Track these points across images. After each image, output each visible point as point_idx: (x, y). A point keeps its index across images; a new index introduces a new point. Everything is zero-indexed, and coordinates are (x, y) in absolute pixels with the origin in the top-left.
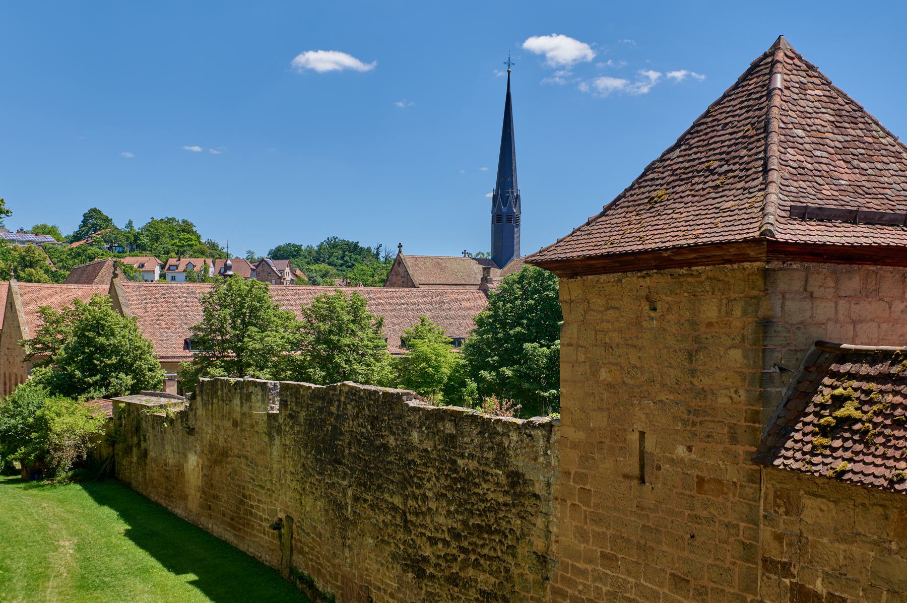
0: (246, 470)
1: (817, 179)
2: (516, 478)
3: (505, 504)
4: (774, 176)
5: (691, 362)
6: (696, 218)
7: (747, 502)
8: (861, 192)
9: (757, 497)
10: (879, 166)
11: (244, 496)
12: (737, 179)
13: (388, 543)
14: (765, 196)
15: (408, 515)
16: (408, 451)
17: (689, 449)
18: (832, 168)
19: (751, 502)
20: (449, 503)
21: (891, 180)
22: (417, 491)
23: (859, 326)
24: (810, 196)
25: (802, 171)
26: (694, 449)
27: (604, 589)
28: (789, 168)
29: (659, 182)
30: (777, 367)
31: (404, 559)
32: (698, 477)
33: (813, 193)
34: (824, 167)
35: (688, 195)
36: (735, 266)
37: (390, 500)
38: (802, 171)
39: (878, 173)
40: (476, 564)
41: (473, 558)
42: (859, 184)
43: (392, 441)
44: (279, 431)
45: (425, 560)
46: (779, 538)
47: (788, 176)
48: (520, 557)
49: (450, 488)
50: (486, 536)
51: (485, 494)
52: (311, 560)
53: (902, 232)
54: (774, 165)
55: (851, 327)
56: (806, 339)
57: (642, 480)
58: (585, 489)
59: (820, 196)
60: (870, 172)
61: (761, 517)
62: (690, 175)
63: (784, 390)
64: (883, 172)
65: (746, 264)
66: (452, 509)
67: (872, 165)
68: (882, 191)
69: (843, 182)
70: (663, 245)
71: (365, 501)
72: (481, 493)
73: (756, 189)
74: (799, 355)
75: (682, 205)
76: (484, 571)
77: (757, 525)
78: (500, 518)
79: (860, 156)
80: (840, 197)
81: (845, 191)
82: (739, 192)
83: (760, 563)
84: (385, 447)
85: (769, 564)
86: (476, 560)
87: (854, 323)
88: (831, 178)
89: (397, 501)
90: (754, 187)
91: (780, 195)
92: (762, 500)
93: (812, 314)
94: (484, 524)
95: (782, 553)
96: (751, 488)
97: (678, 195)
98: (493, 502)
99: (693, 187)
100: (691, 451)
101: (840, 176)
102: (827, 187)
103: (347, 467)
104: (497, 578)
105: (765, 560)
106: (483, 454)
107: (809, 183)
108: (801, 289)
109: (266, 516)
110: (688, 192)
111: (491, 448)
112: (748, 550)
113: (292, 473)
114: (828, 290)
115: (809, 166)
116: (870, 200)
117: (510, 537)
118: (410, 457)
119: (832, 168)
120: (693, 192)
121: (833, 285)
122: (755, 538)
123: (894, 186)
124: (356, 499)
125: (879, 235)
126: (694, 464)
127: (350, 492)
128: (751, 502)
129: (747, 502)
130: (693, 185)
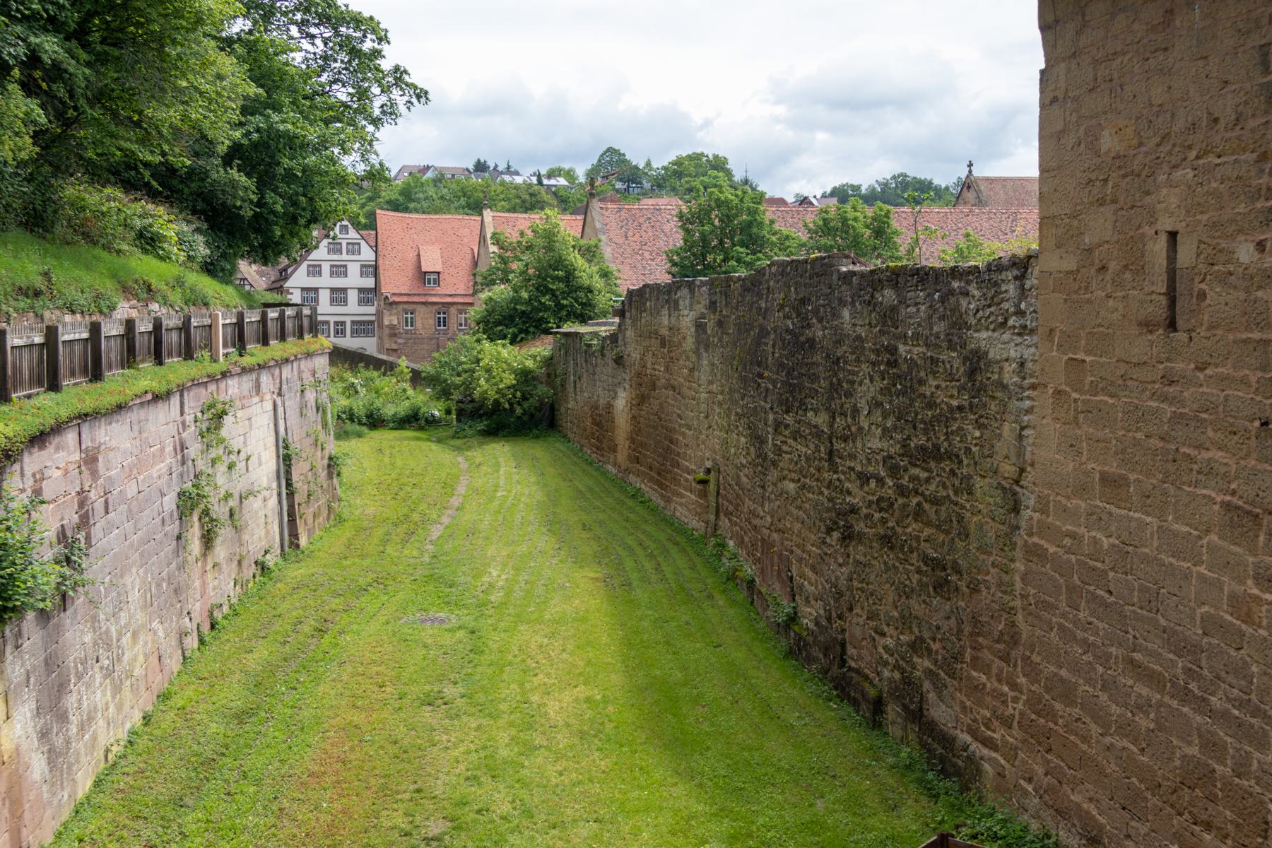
0: (673, 406)
2: (976, 362)
3: (960, 408)
11: (671, 441)
20: (885, 415)
27: (1106, 542)
40: (918, 513)
41: (915, 501)
45: (854, 510)
48: (978, 493)
49: (885, 391)
50: (932, 464)
51: (932, 393)
52: (736, 524)
57: (1172, 325)
58: (1075, 360)
66: (889, 424)
72: (928, 394)
76: (928, 524)
78: (952, 432)
86: (919, 504)
94: (930, 444)
98: (943, 406)
100: (1263, 251)
104: (947, 533)
106: (931, 329)
109: (693, 467)
111: (942, 318)
117: (966, 462)
124: (778, 425)
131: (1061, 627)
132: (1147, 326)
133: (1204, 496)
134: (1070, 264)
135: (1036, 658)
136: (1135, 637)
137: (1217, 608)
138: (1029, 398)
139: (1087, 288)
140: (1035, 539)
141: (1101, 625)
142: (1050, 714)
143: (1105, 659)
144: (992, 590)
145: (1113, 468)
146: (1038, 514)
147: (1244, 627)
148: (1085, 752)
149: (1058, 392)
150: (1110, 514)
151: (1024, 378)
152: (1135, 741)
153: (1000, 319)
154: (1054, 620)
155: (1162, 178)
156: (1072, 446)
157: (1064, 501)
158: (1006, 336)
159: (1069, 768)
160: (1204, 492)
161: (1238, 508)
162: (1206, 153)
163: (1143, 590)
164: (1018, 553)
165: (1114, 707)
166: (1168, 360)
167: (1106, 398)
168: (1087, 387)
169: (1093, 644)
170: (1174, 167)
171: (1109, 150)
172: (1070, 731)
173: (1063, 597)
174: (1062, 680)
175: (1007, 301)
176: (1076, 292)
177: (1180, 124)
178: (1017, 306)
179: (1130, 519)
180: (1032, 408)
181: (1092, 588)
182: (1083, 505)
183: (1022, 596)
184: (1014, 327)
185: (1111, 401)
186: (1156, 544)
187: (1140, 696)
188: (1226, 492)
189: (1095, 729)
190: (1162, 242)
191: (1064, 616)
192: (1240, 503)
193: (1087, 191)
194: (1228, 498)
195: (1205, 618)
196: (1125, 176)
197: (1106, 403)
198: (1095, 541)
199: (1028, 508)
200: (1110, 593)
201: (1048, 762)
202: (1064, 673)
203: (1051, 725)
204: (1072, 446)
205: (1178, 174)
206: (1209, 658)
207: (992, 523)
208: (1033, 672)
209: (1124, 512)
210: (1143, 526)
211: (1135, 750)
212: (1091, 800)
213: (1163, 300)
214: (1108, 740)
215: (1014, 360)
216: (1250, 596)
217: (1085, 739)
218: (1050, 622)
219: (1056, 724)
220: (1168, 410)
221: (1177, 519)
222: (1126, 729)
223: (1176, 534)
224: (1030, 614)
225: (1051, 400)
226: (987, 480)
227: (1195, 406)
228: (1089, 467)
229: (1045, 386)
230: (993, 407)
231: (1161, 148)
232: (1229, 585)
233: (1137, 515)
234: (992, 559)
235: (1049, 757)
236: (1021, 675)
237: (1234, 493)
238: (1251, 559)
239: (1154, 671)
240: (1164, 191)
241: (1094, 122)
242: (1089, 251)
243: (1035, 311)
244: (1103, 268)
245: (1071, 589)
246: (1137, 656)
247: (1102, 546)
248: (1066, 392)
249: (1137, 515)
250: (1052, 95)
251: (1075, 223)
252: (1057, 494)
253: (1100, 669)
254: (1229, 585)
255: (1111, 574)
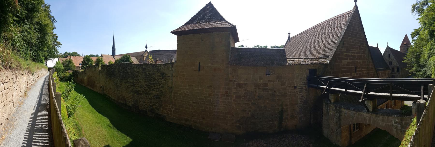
13: (130, 89)
15: (134, 83)
16: (134, 72)
22: (137, 79)
31: (134, 91)
37: (129, 81)
43: (129, 71)
44: (101, 73)
71: (123, 82)
84: (128, 72)
89: (131, 81)
103: (118, 77)
113: (104, 79)
118: (134, 73)
124: (121, 82)
127: (119, 81)
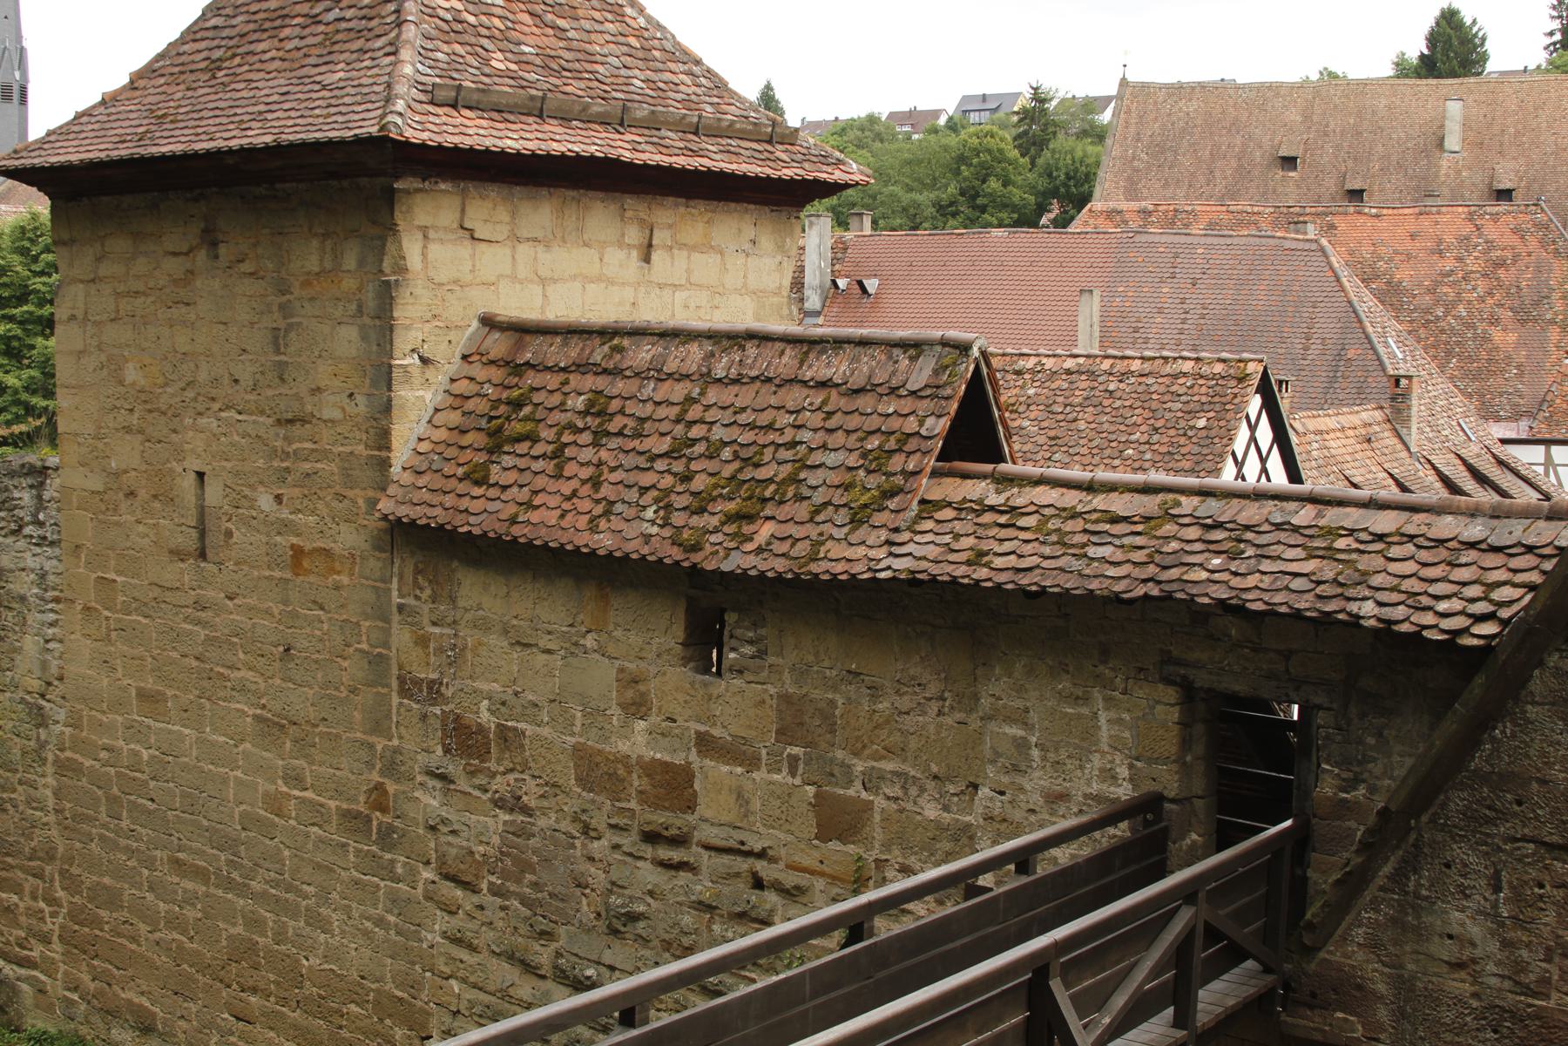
1: (485, 42)
4: (410, 32)
5: (278, 351)
6: (283, 98)
7: (370, 582)
8: (556, 67)
9: (388, 574)
10: (587, 25)
12: (353, 35)
14: (394, 64)
17: (278, 499)
18: (510, 24)
19: (378, 584)
21: (605, 51)
23: (550, 289)
24: (471, 70)
25: (459, 27)
26: (285, 499)
27: (145, 754)
28: (437, 20)
29: (225, 33)
30: (416, 356)
32: (292, 546)
33: (476, 64)
34: (497, 22)
35: (273, 59)
36: (345, 183)
38: (459, 27)
39: (585, 37)
42: (553, 53)
46: (422, 641)
47: (434, 33)
53: (617, 136)
54: (411, 14)
55: (538, 290)
56: (465, 308)
57: (202, 555)
59: (487, 70)
60: (572, 34)
61: (395, 609)
62: (278, 23)
63: (428, 396)
64: (593, 36)
65: (363, 181)
67: (575, 24)
68: (588, 67)
69: (526, 49)
70: (226, 143)
73: (381, 53)
74: (452, 336)
75: (262, 75)
77: (387, 620)
79: (557, 7)
80: (521, 73)
81: (527, 63)
82: (355, 56)
83: (395, 684)
85: (408, 687)
87: (543, 282)
88: (506, 40)
90: (379, 49)
91: (419, 65)
92: (395, 580)
93: (474, 266)
95: (428, 664)
96: (379, 559)
97: (256, 58)
99: (282, 45)
100: (280, 503)
101: (522, 38)
102: (499, 55)
105: (402, 680)
107: (469, 48)
108: (455, 225)
110: (273, 53)
112: (378, 662)
114: (498, 227)
115: (471, 19)
116: (570, 81)
119: (510, 24)
120: (281, 54)
121: (507, 219)
122: (386, 645)
123: (610, 59)
125: (580, 138)
126: (285, 527)
128: (378, 584)
129: (370, 582)
130: (281, 40)
131: (102, 838)
132: (178, 554)
133: (238, 710)
134: (96, 483)
135: (75, 870)
136: (180, 839)
137: (252, 805)
138: (52, 610)
139: (115, 510)
140: (68, 754)
141: (144, 831)
142: (96, 922)
143: (150, 864)
144: (21, 808)
145: (150, 684)
146: (70, 729)
147: (276, 819)
148: (133, 951)
149: (87, 609)
150: (149, 727)
151: (46, 590)
152: (184, 932)
153: (13, 526)
154: (94, 831)
155: (188, 421)
156: (105, 662)
157: (99, 715)
158: (22, 544)
159: (118, 968)
160: (238, 706)
161: (268, 720)
162: (228, 408)
163: (184, 796)
164: (50, 769)
165: (161, 904)
166: (200, 587)
167: (140, 618)
168: (119, 607)
169: (137, 849)
170: (200, 414)
171: (134, 384)
172: (119, 935)
173: (103, 809)
174: (105, 887)
175: (22, 508)
176: (104, 513)
177: (203, 376)
178: (35, 515)
179: (170, 732)
180: (57, 621)
181: (132, 798)
182: (120, 719)
183: (57, 811)
184: (31, 537)
185: (144, 621)
186: (194, 753)
187: (185, 891)
188: (258, 706)
189: (143, 928)
190: (190, 480)
191: (105, 826)
192: (269, 715)
193: (111, 416)
194: (259, 711)
195: (244, 815)
196: (150, 411)
197: (139, 622)
198: (136, 754)
199: (58, 722)
200: (152, 800)
201: (94, 967)
202: (107, 880)
203: (97, 932)
204: (105, 662)
205: (203, 421)
206: (246, 849)
207: (17, 740)
208: (72, 885)
209: (162, 725)
210: (181, 738)
211: (185, 939)
212: (142, 993)
213: (194, 534)
214: (158, 935)
215: (33, 571)
216: (281, 793)
217: (134, 939)
218: (90, 834)
219: (102, 930)
220: (202, 633)
221: (215, 730)
222: (174, 922)
223: (213, 744)
224: (66, 828)
225: (80, 616)
226: (8, 695)
227: (226, 631)
228: (125, 682)
229: (72, 601)
230: (10, 619)
231: (186, 393)
232: (263, 785)
233: (176, 728)
234: (18, 776)
235: (95, 962)
236: (59, 889)
237: (264, 707)
238: (281, 762)
239: (197, 867)
240: (191, 434)
241: (116, 351)
242: (117, 475)
243: (55, 524)
244: (132, 493)
245: (113, 800)
246: (181, 855)
247: (141, 758)
248: (96, 609)
249: (176, 728)
250: (70, 312)
251: (101, 446)
252: (91, 709)
253: (146, 872)
254: (263, 785)
255: (152, 784)
